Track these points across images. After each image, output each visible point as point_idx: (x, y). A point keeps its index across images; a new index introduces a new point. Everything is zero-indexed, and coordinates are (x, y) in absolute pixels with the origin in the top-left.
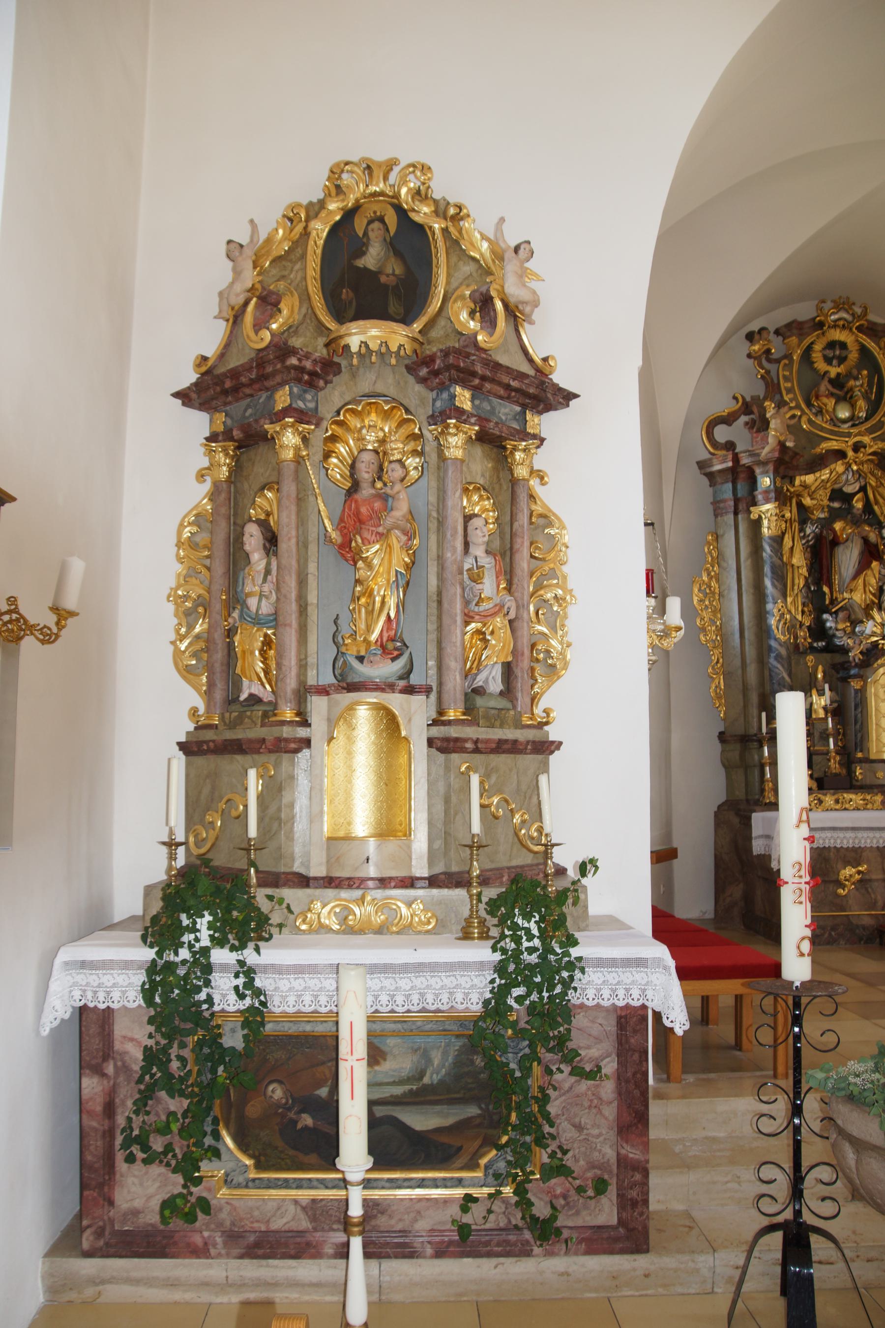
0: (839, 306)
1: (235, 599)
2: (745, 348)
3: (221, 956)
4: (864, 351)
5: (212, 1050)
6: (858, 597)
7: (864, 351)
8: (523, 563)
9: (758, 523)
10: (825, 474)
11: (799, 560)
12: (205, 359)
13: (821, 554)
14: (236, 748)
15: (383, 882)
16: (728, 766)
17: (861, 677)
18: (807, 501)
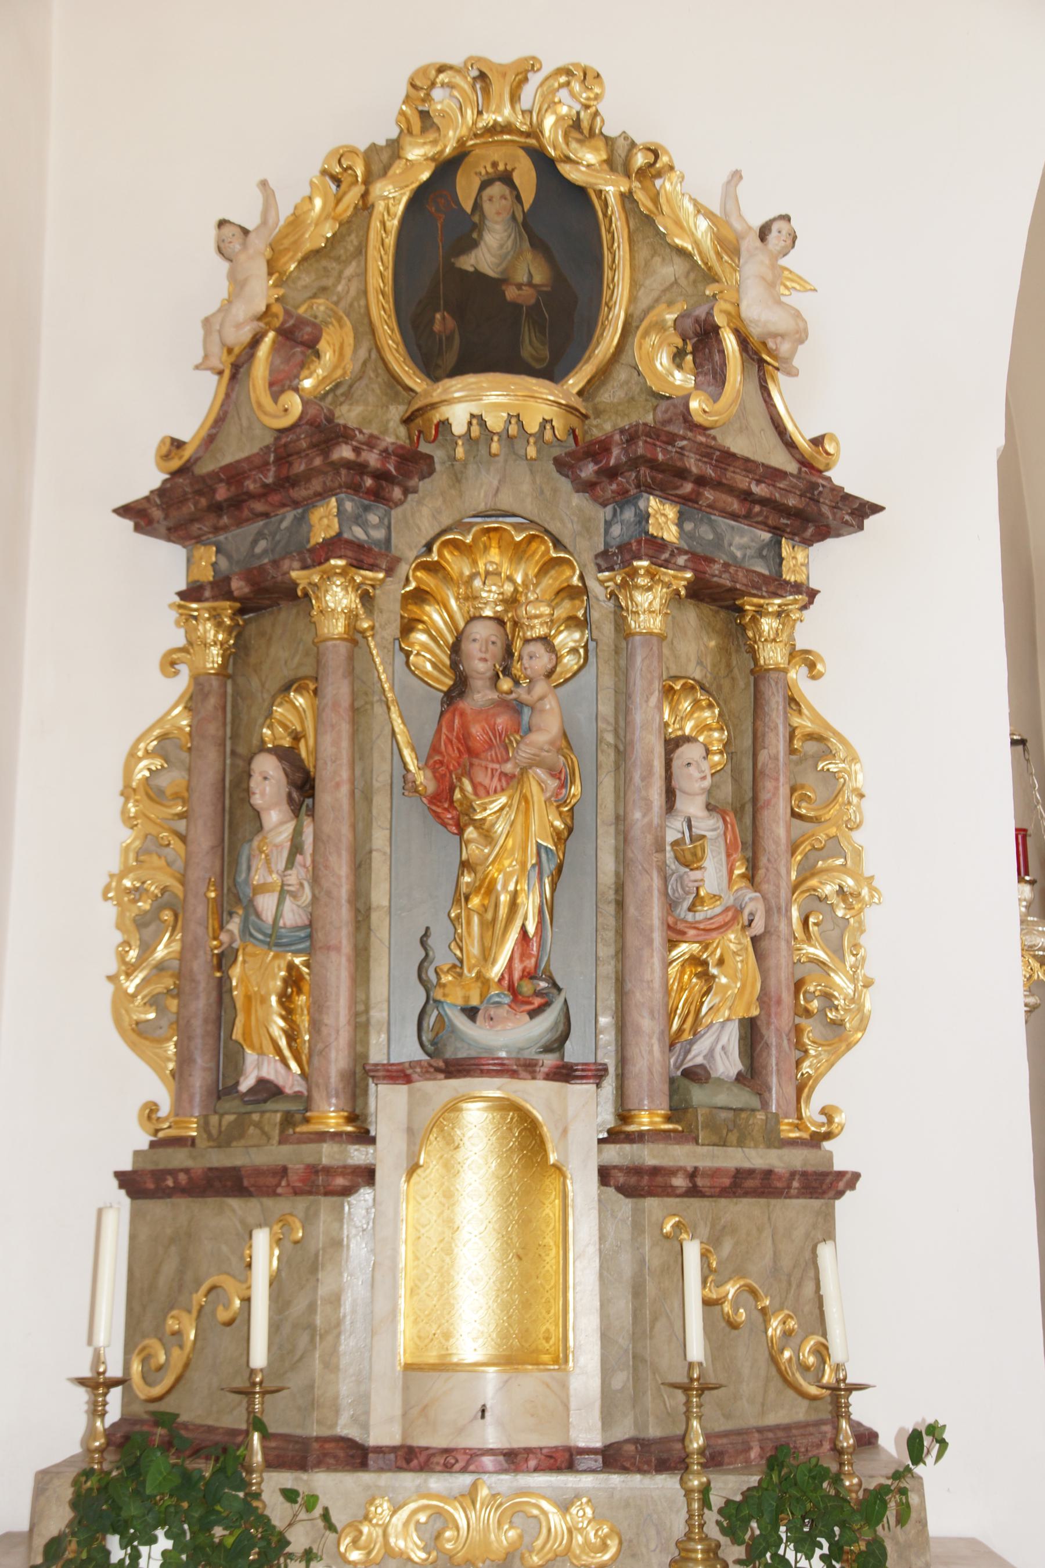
1: (232, 896)
8: (777, 827)
12: (177, 444)
14: (230, 1183)
15: (513, 1459)
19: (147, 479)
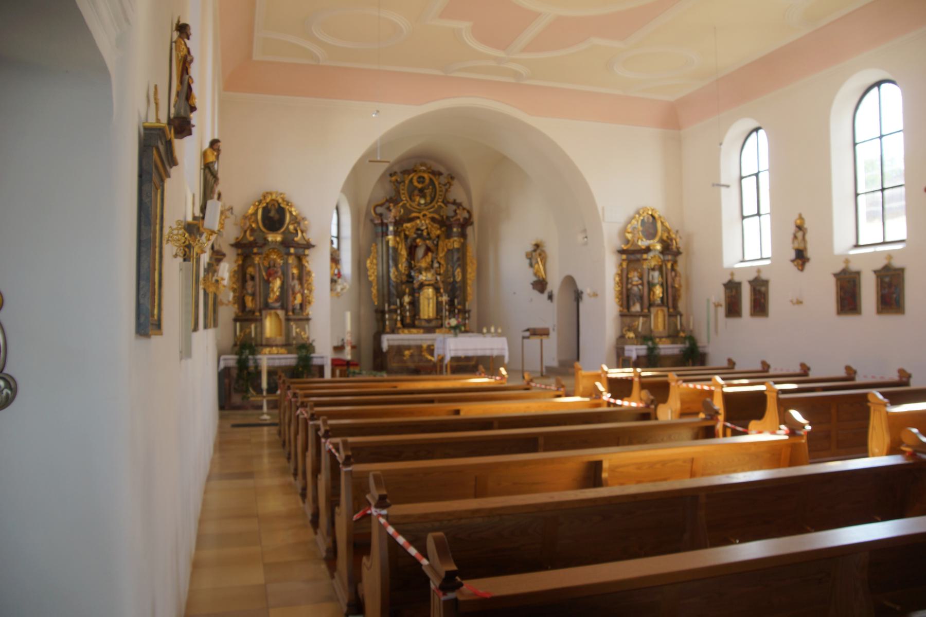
0: (422, 165)
2: (389, 178)
3: (250, 357)
4: (431, 180)
5: (249, 374)
6: (423, 264)
9: (388, 242)
11: (404, 253)
13: (412, 250)
14: (247, 320)
16: (378, 320)
18: (407, 233)
19: (233, 241)
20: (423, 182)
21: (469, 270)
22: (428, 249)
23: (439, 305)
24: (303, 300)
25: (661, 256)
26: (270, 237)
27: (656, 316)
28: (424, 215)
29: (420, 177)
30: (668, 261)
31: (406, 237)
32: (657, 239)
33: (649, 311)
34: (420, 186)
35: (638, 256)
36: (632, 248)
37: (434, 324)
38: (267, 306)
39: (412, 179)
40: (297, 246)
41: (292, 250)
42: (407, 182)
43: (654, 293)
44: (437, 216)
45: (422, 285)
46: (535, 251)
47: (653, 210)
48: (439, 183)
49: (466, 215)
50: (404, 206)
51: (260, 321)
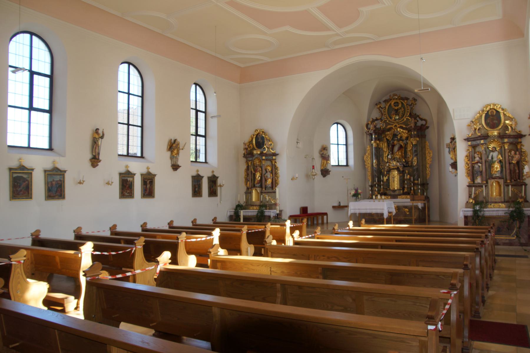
4: (402, 103)
6: (398, 157)
7: (402, 103)
10: (391, 132)
13: (391, 147)
17: (389, 174)
18: (387, 137)
20: (398, 106)
21: (428, 158)
22: (401, 147)
23: (402, 182)
24: (272, 183)
25: (500, 140)
26: (255, 152)
27: (492, 185)
28: (396, 126)
29: (395, 103)
30: (504, 143)
31: (387, 140)
32: (500, 127)
33: (487, 183)
34: (396, 108)
35: (478, 142)
36: (473, 137)
37: (397, 193)
38: (254, 186)
39: (390, 104)
40: (266, 155)
41: (264, 158)
42: (387, 107)
43: (493, 167)
44: (404, 126)
45: (389, 171)
46: (451, 142)
47: (494, 105)
48: (407, 104)
49: (424, 122)
50: (385, 121)
51: (251, 193)
